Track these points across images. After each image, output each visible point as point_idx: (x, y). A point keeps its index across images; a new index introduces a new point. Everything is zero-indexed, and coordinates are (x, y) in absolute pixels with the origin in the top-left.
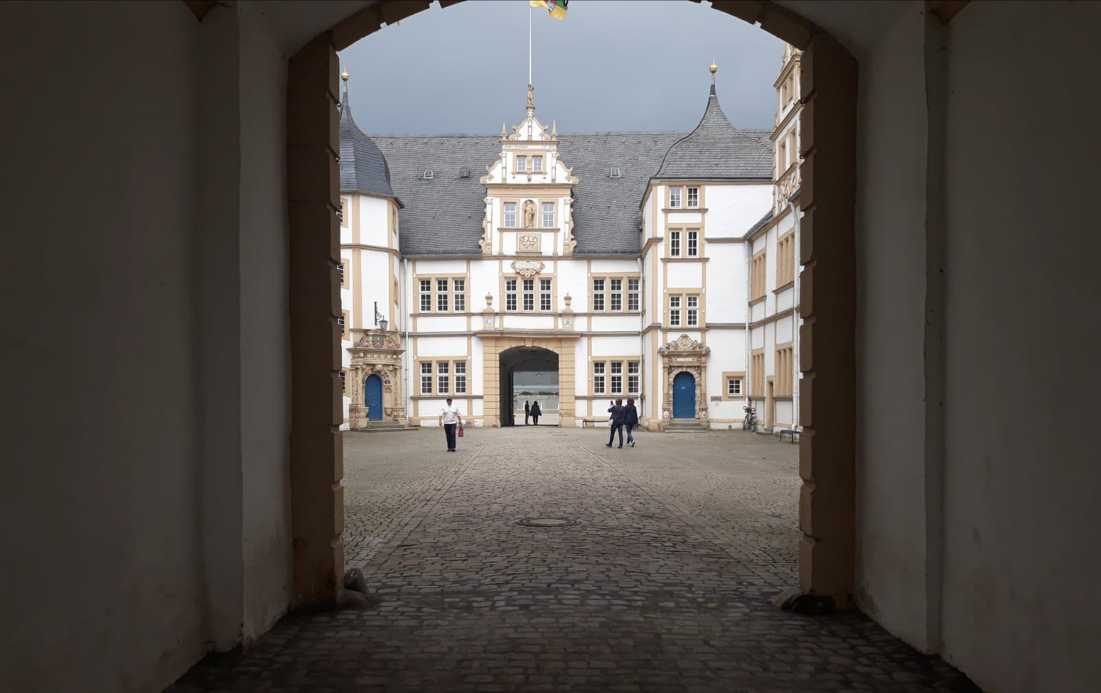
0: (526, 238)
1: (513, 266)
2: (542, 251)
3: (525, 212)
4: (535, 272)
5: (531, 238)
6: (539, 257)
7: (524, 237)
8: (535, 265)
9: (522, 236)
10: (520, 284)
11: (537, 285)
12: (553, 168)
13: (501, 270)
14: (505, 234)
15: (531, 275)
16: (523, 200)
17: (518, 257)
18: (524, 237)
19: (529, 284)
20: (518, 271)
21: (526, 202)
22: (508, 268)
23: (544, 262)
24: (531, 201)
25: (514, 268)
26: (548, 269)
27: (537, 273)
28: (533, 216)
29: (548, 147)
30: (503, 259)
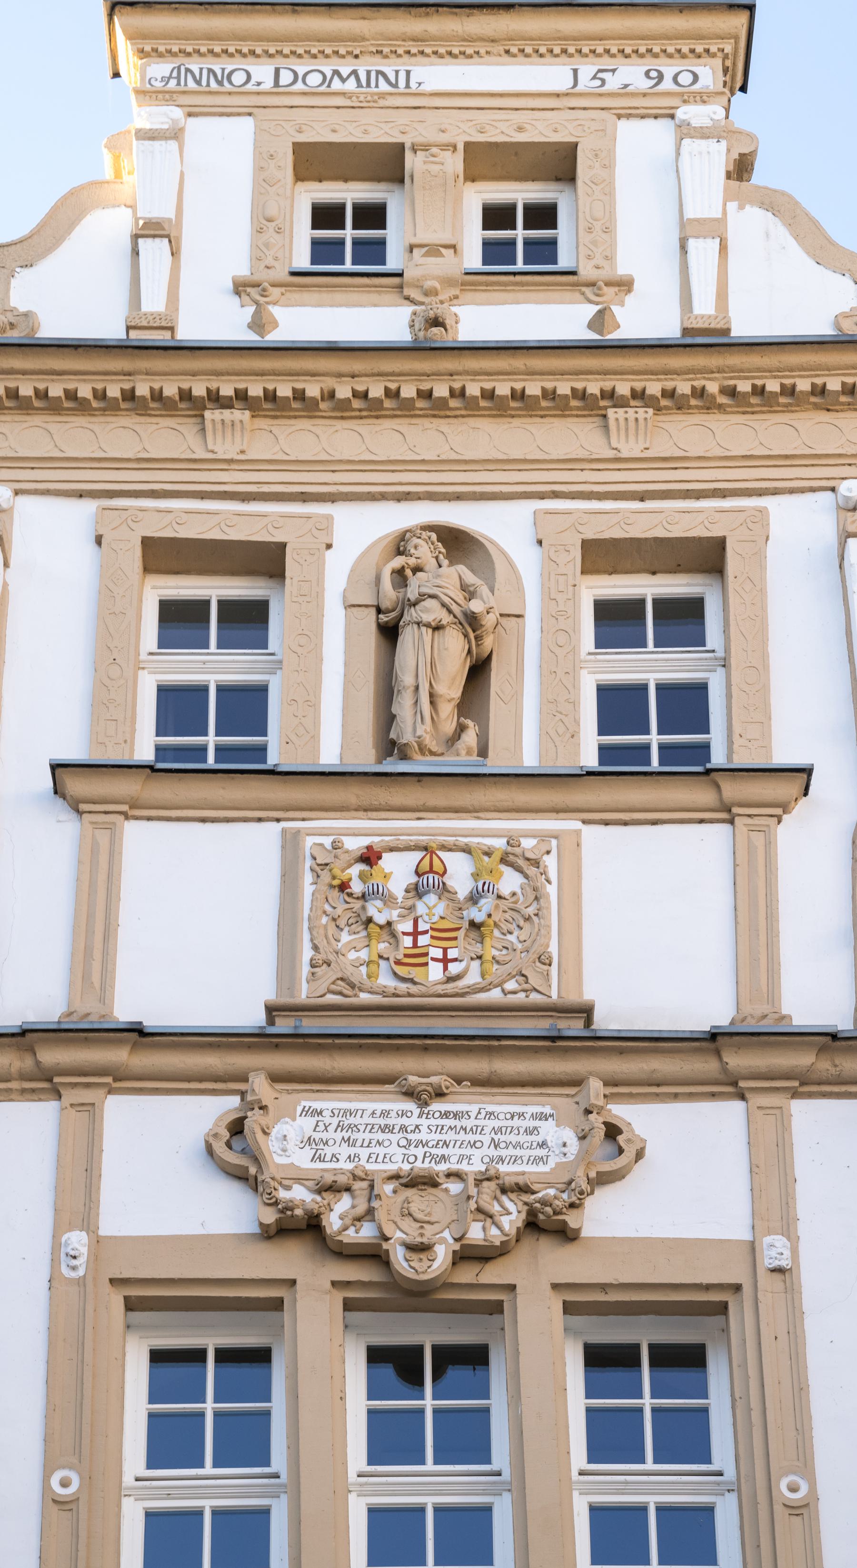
0: (398, 870)
1: (237, 1154)
2: (591, 991)
3: (390, 633)
4: (511, 1216)
5: (459, 872)
6: (554, 1041)
7: (369, 858)
8: (521, 1135)
9: (355, 844)
10: (327, 1380)
11: (545, 1383)
12: (687, 232)
13: (78, 1189)
14: (152, 849)
15: (468, 1255)
16: (358, 533)
17: (304, 1042)
18: (369, 858)
19: (431, 1363)
20: (300, 1195)
21: (400, 545)
22: (161, 1177)
23: (630, 1114)
24: (456, 543)
25: (248, 1175)
26: (681, 1187)
27: (547, 1226)
28: (478, 671)
29: (631, 75)
30: (121, 1080)
